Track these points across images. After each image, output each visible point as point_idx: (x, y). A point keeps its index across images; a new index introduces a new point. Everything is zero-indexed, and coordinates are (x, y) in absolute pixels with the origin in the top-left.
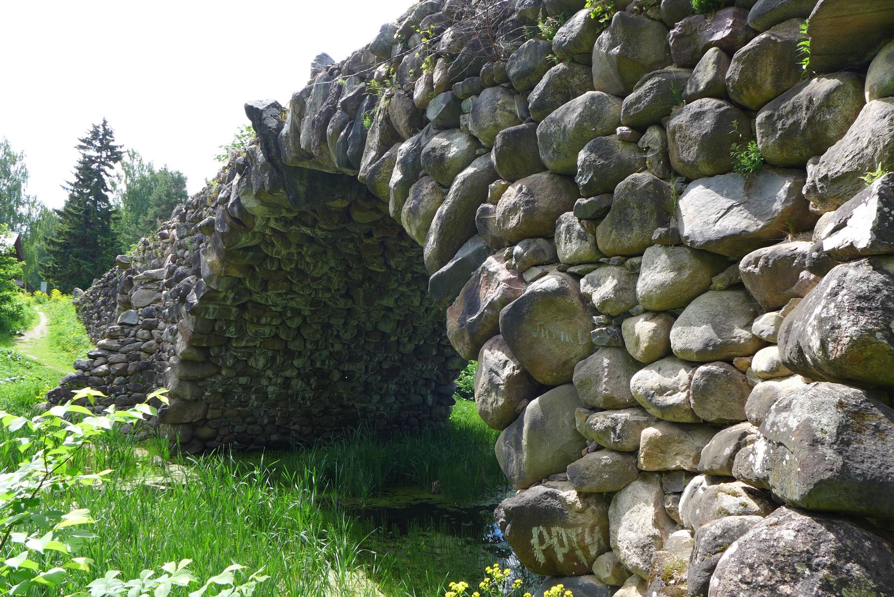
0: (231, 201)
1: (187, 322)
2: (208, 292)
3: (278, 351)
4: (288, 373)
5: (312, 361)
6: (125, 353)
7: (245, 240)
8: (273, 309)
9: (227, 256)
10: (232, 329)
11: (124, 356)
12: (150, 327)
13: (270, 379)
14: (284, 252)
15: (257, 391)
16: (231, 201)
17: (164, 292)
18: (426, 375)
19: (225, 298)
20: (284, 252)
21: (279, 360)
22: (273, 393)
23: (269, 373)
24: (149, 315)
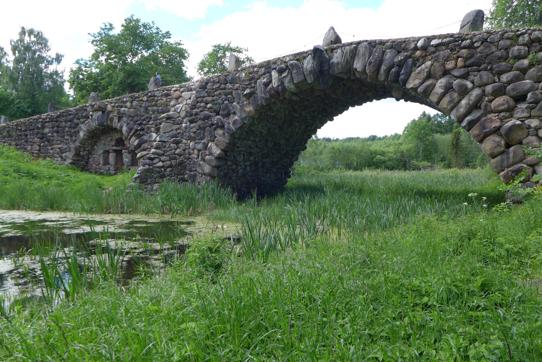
8: (256, 132)
11: (168, 158)
24: (175, 136)
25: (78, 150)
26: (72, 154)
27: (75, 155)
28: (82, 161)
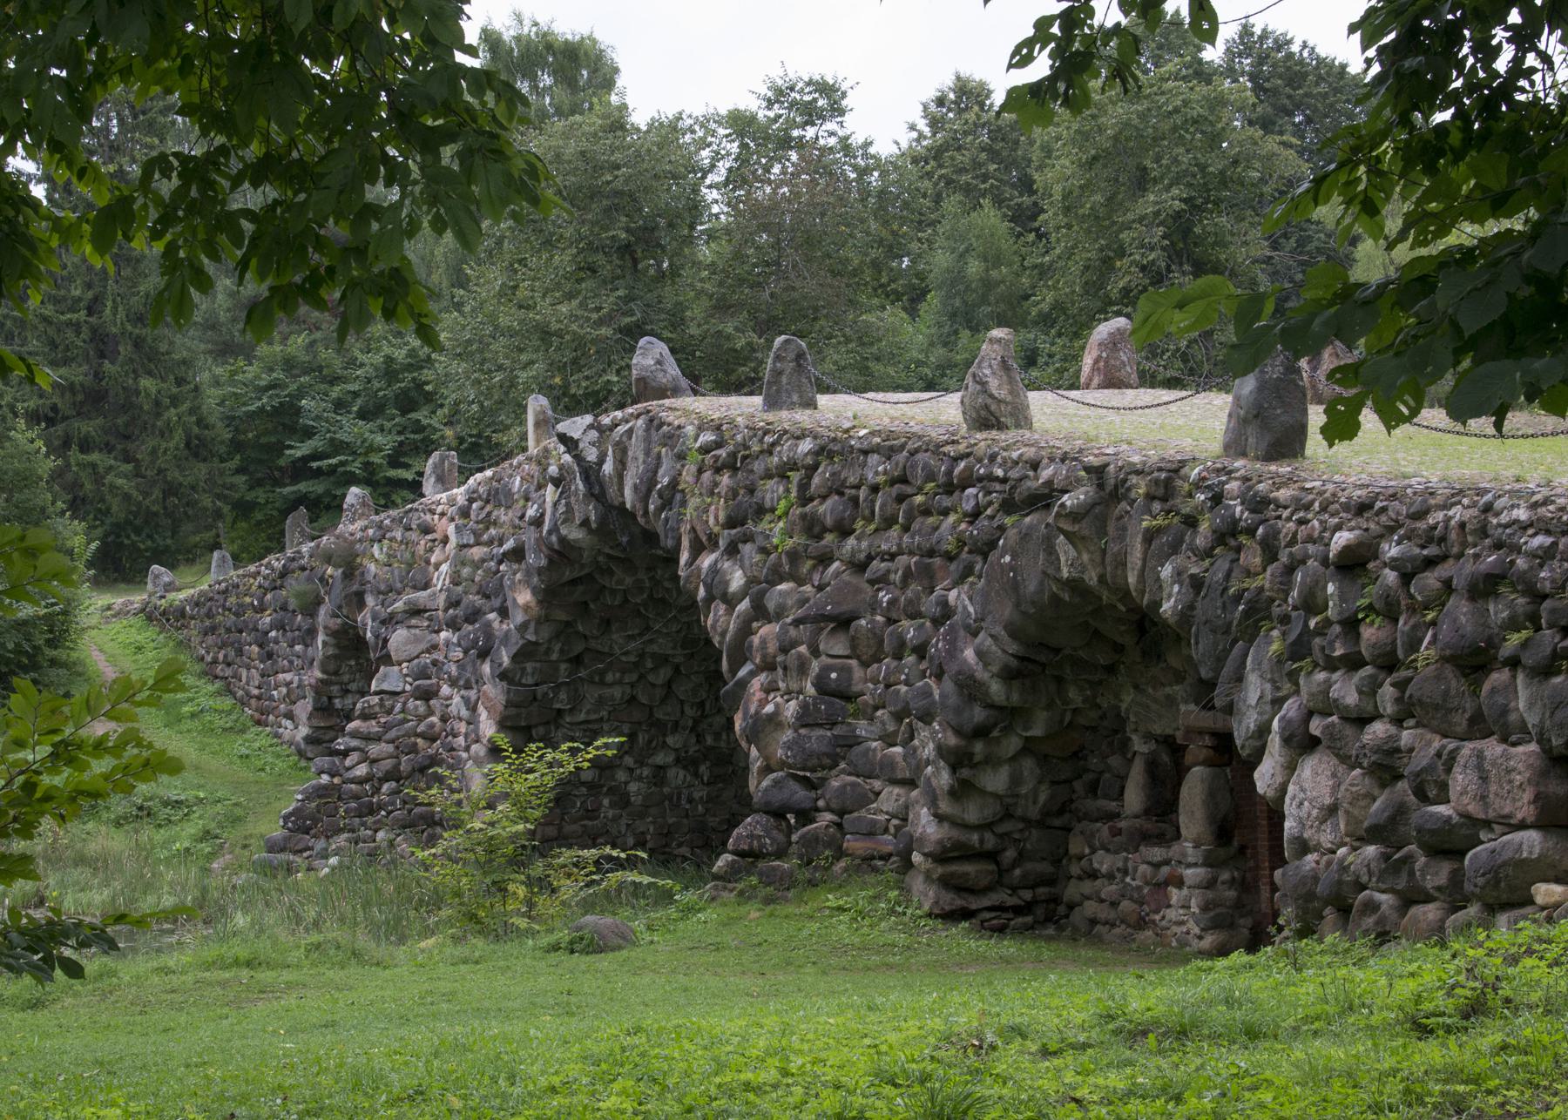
0: (546, 528)
1: (494, 691)
2: (523, 646)
3: (640, 723)
4: (660, 759)
5: (698, 736)
6: (392, 741)
7: (568, 575)
8: (624, 658)
9: (548, 595)
10: (563, 696)
12: (427, 695)
13: (631, 770)
14: (629, 581)
15: (612, 791)
16: (546, 528)
17: (443, 635)
19: (548, 651)
20: (629, 581)
21: (642, 738)
22: (638, 793)
23: (629, 761)
24: (423, 674)
25: (320, 689)
26: (310, 708)
27: (315, 709)
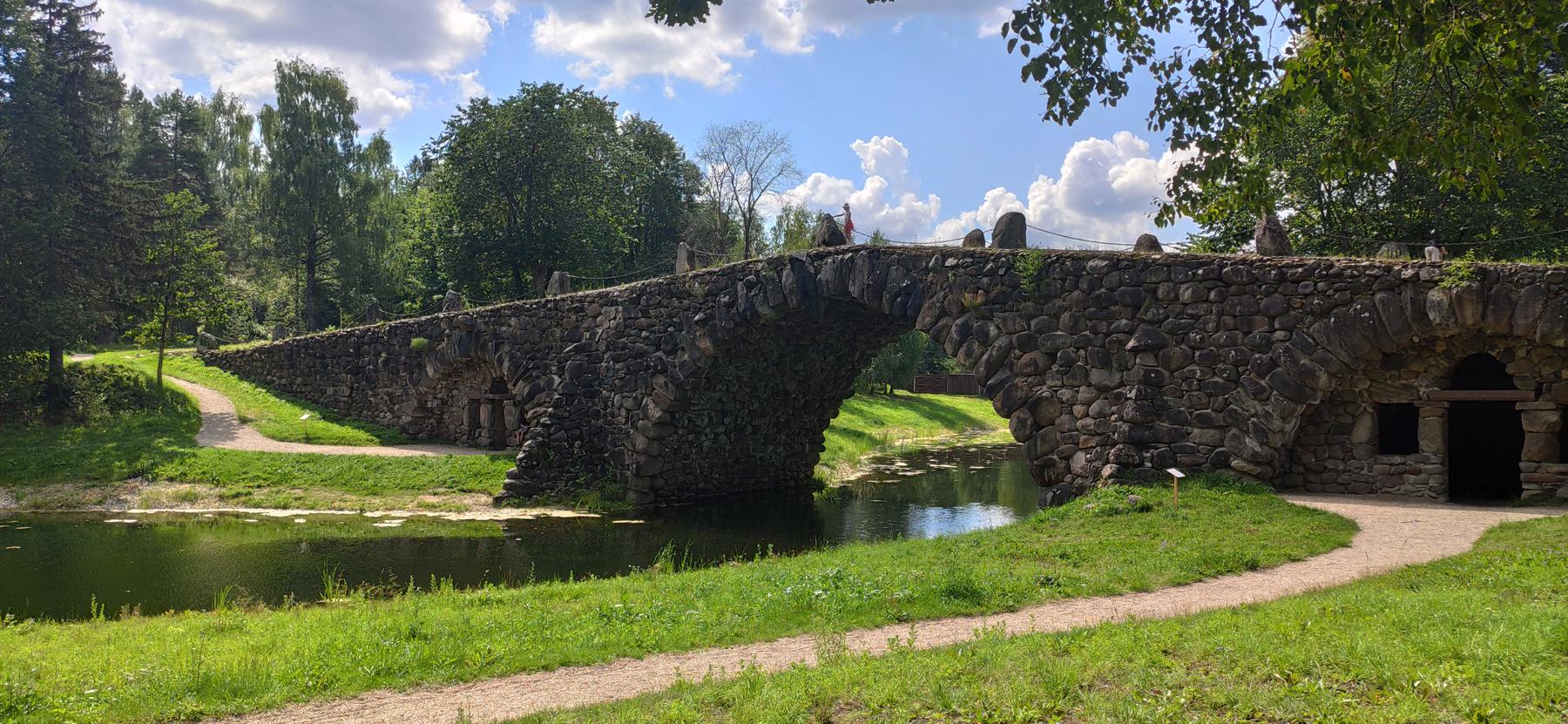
18: (808, 426)
28: (430, 418)
